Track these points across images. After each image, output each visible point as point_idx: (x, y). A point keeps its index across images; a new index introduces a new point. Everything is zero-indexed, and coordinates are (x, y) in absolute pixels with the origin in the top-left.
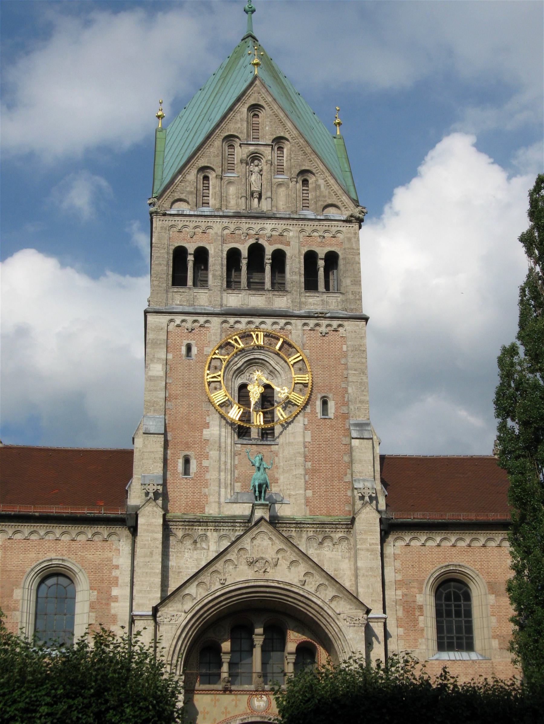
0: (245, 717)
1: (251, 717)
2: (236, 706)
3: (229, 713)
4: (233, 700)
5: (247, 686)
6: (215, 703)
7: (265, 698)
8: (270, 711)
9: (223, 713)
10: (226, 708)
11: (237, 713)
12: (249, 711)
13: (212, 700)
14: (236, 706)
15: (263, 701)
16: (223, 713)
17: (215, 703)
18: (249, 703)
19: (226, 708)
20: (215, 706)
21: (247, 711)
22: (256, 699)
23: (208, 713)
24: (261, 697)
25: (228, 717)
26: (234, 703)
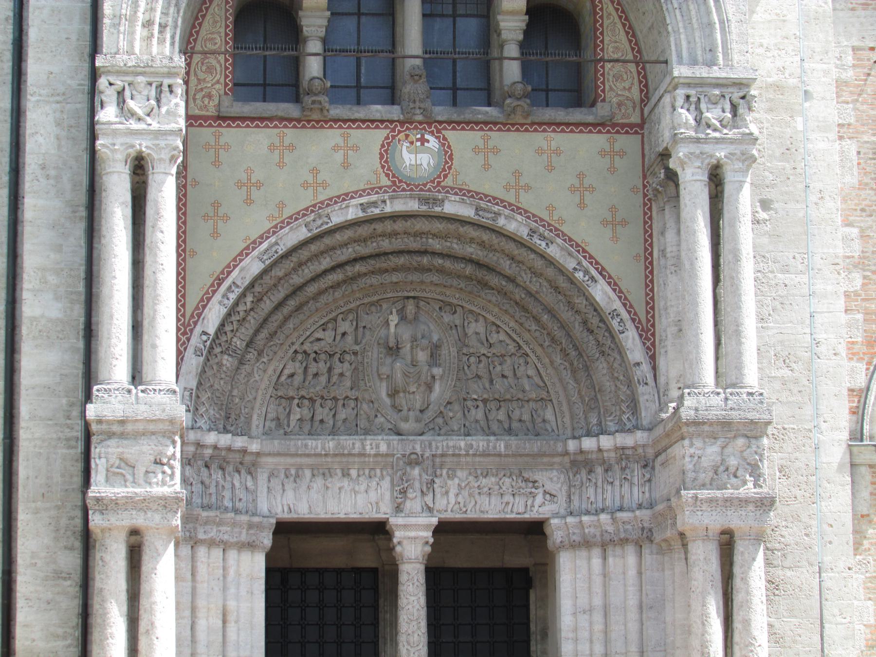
0: (374, 198)
1: (392, 198)
2: (346, 165)
3: (325, 185)
4: (336, 148)
5: (379, 107)
6: (282, 157)
7: (433, 143)
8: (449, 182)
9: (305, 185)
10: (315, 171)
11: (348, 186)
12: (385, 181)
13: (272, 148)
14: (346, 165)
15: (429, 151)
16: (305, 185)
17: (282, 157)
18: (386, 154)
19: (315, 171)
20: (281, 165)
21: (378, 179)
22: (406, 144)
23: (259, 185)
24: (423, 141)
25: (321, 198)
26: (339, 157)
